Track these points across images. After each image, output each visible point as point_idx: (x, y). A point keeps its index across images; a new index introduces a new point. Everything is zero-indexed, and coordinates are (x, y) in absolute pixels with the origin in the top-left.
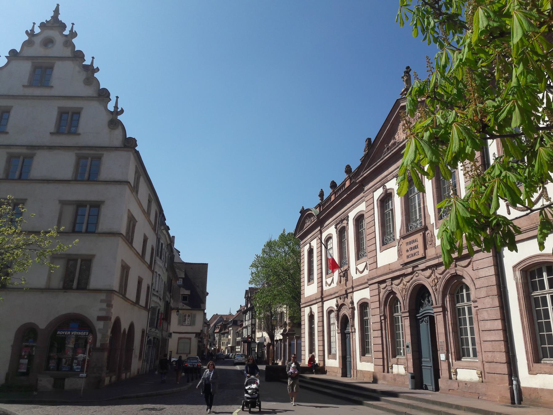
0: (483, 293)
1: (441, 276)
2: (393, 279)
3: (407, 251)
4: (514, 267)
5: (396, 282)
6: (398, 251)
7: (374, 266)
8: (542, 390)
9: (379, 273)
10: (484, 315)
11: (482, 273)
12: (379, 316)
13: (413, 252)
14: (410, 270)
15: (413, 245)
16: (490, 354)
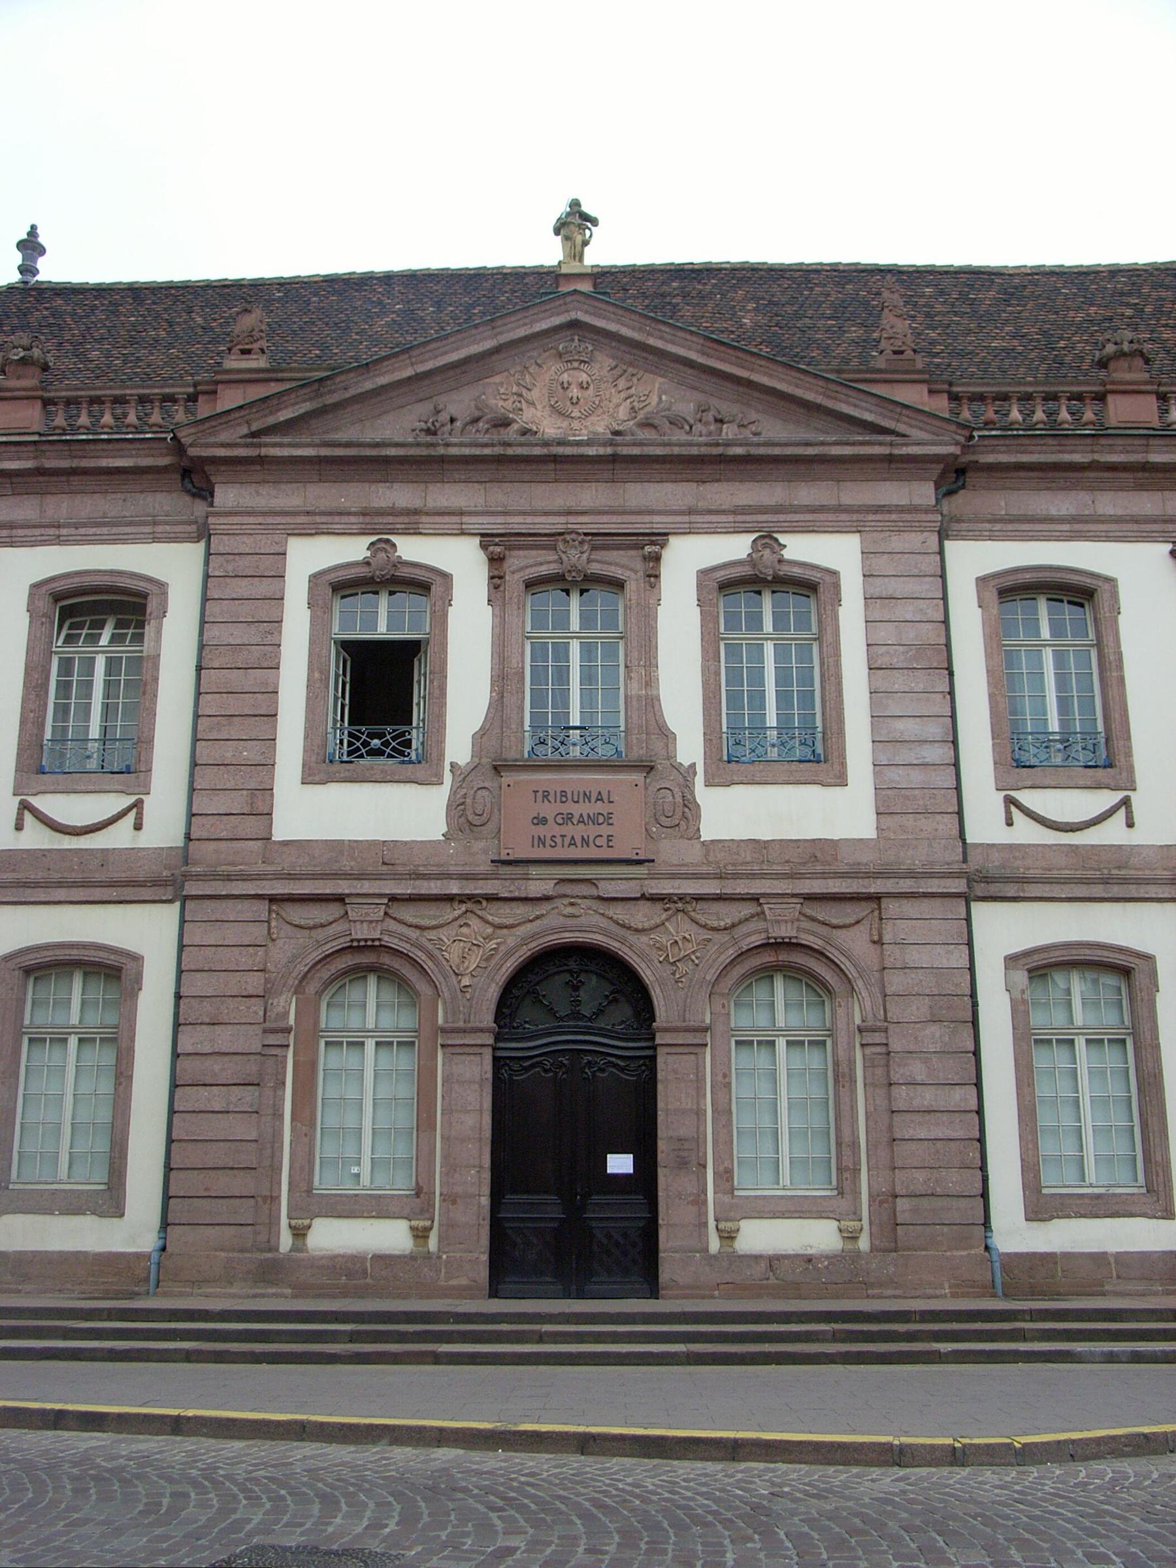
0: (917, 1009)
1: (723, 937)
2: (393, 898)
3: (544, 821)
4: (1012, 961)
5: (408, 913)
6: (457, 808)
7: (250, 826)
8: (1067, 1256)
9: (286, 862)
10: (918, 1070)
11: (915, 957)
12: (258, 1030)
13: (578, 831)
14: (535, 888)
15: (599, 807)
16: (920, 1176)
